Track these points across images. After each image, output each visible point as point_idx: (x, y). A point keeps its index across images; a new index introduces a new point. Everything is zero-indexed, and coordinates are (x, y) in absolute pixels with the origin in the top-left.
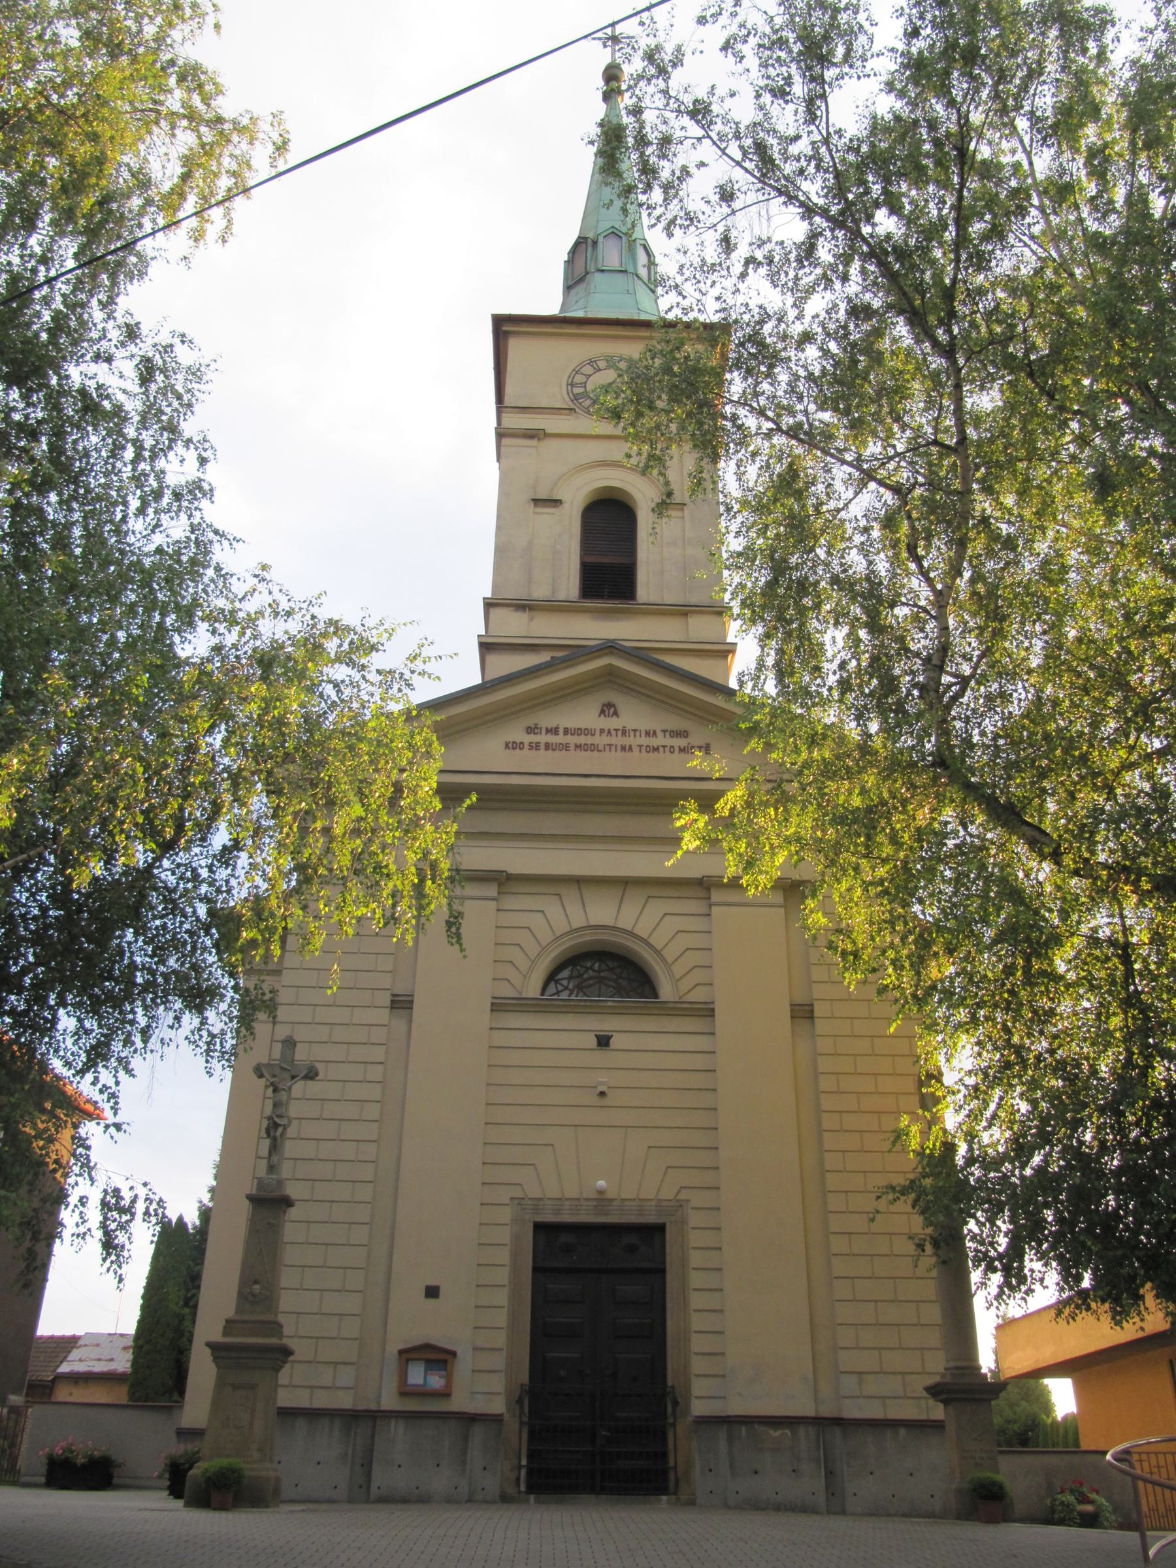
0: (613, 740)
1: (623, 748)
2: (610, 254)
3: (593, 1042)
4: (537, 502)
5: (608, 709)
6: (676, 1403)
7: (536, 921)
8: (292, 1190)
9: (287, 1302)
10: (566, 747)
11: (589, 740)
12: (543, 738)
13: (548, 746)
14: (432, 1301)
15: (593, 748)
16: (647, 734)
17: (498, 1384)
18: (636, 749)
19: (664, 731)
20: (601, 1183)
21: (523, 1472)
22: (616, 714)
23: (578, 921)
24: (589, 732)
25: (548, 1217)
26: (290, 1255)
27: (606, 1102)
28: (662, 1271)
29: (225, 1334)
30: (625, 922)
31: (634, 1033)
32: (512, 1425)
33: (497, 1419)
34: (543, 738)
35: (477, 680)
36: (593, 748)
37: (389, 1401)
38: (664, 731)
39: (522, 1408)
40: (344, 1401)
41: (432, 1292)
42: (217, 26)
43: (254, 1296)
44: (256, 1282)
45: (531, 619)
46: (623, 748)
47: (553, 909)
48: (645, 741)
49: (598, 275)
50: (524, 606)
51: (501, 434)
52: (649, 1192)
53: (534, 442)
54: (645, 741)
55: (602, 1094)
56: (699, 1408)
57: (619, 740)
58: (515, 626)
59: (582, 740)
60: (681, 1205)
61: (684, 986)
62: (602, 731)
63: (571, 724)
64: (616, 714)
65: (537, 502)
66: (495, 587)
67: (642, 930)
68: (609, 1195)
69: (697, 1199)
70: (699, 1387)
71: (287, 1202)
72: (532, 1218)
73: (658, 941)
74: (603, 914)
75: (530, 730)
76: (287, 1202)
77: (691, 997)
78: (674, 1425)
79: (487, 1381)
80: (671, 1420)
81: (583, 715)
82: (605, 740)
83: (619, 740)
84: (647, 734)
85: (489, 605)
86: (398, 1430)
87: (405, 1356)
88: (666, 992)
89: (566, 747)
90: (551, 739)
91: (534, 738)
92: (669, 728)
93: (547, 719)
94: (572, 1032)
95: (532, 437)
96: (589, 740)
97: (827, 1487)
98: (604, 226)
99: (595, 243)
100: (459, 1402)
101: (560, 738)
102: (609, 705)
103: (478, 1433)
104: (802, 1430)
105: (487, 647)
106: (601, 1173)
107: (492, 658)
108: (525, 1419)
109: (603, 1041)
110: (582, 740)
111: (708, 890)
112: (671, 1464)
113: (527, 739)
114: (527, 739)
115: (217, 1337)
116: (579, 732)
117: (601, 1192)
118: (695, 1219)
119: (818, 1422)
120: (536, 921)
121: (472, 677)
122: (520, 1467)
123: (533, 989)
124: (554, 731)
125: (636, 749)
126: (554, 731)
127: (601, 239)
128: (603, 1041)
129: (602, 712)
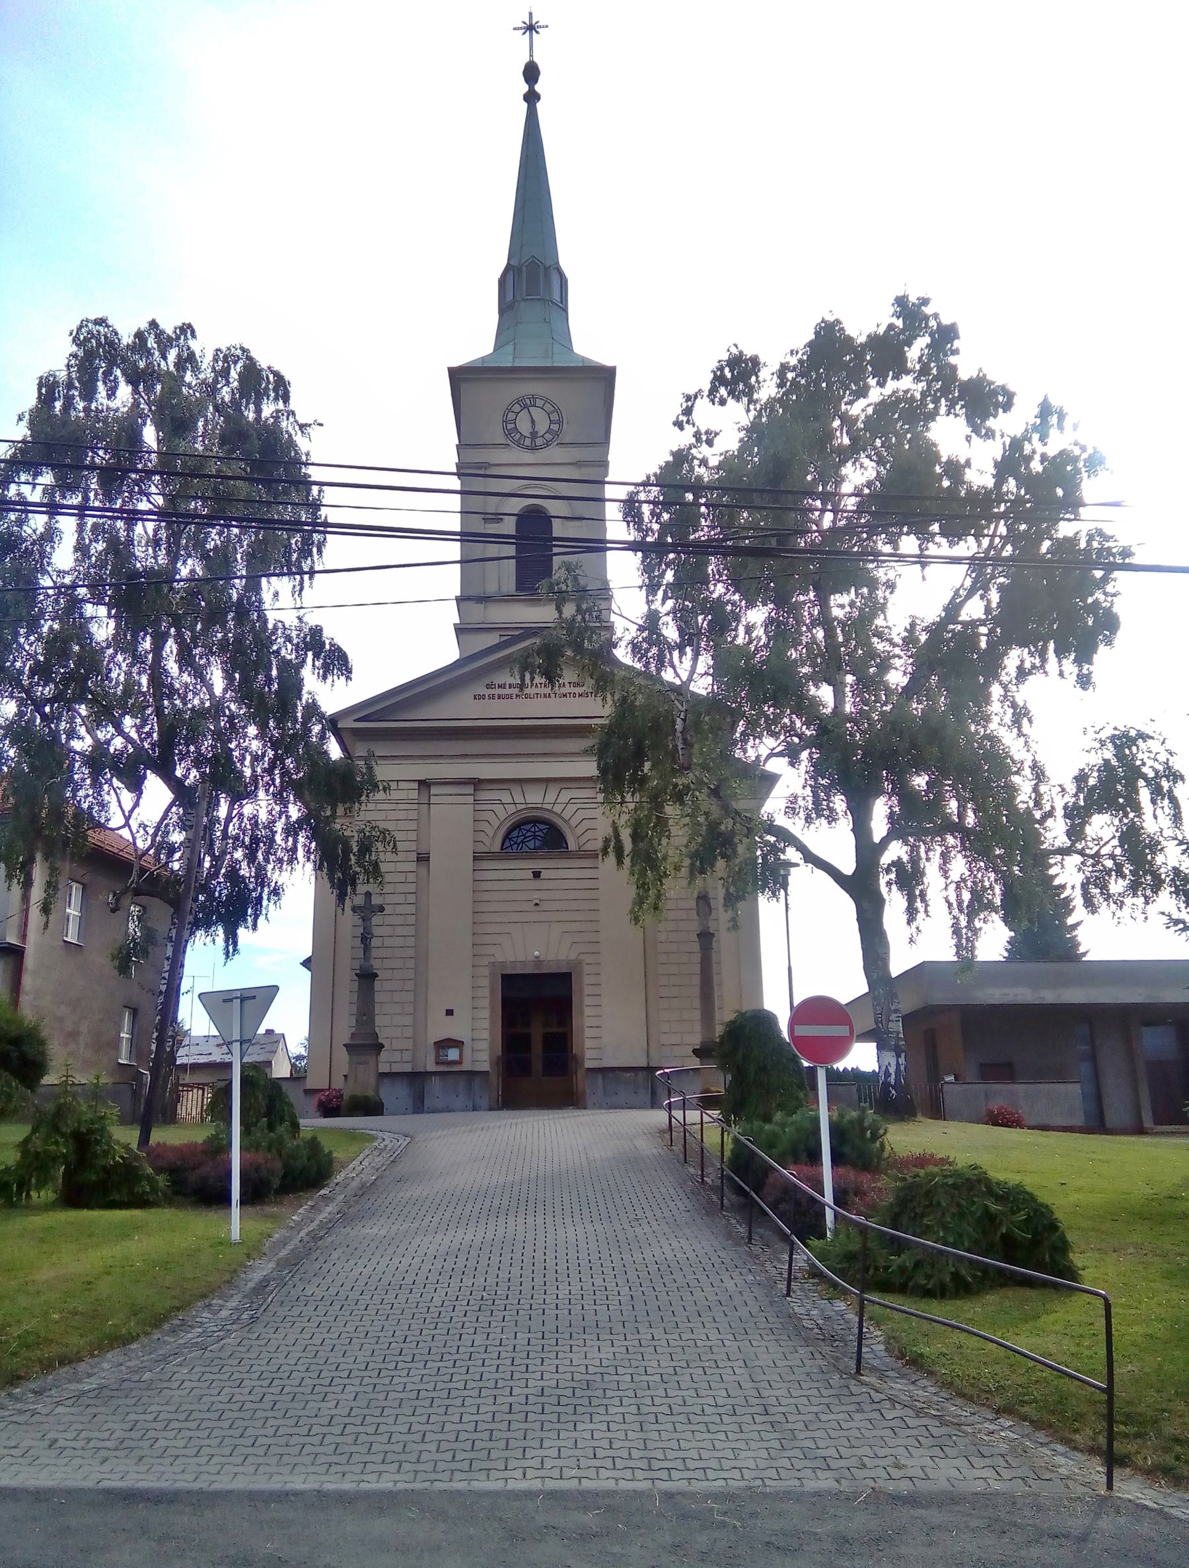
6: (577, 1063)
9: (379, 1021)
17: (485, 1056)
20: (537, 953)
25: (509, 972)
26: (378, 998)
31: (555, 870)
32: (495, 1079)
37: (431, 1067)
41: (450, 1013)
46: (545, 696)
50: (484, 599)
52: (562, 957)
55: (537, 904)
56: (589, 1064)
60: (579, 963)
61: (583, 840)
70: (589, 1054)
74: (534, 797)
75: (488, 687)
86: (436, 1082)
88: (572, 845)
91: (491, 691)
100: (466, 1066)
103: (477, 1082)
105: (460, 630)
106: (534, 947)
109: (537, 875)
123: (497, 847)
128: (537, 875)
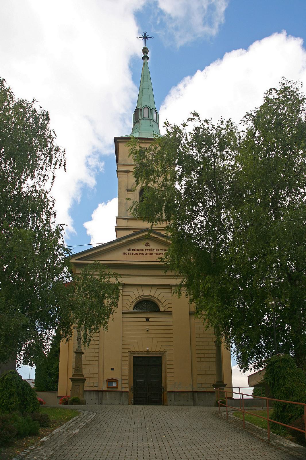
0: (148, 252)
1: (151, 254)
2: (145, 113)
3: (145, 320)
4: (128, 190)
5: (147, 244)
6: (164, 389)
7: (131, 294)
8: (83, 350)
9: (84, 371)
10: (137, 254)
11: (143, 252)
12: (132, 252)
13: (133, 254)
14: (112, 371)
15: (144, 254)
16: (157, 250)
17: (127, 386)
18: (154, 254)
19: (161, 250)
20: (147, 348)
21: (133, 401)
22: (149, 245)
23: (141, 294)
24: (142, 250)
25: (137, 355)
26: (83, 363)
27: (149, 332)
28: (160, 365)
29: (73, 376)
30: (152, 294)
31: (154, 319)
32: (130, 393)
33: (127, 392)
34: (132, 252)
35: (115, 238)
36: (144, 254)
37: (105, 389)
38: (161, 250)
39: (132, 390)
40: (96, 389)
41: (113, 369)
42: (56, 211)
43: (78, 370)
44: (78, 367)
45: (128, 222)
46: (151, 254)
47: (136, 291)
48: (156, 252)
49: (142, 120)
50: (126, 218)
51: (118, 171)
52: (158, 350)
53: (127, 174)
54: (156, 252)
55: (147, 331)
56: (168, 390)
57: (150, 252)
58: (124, 223)
59: (141, 252)
60: (165, 352)
61: (166, 308)
62: (146, 250)
63: (138, 248)
64: (149, 245)
65: (128, 190)
66: (119, 213)
67: (156, 296)
68: (150, 351)
69: (168, 351)
70: (168, 386)
71: (83, 353)
72: (133, 355)
73: (159, 298)
74: (147, 292)
75: (128, 250)
76: (83, 353)
77: (167, 310)
78: (163, 393)
79: (125, 384)
80: (163, 392)
81: (141, 246)
82: (147, 252)
83: (150, 252)
84: (157, 250)
85: (117, 218)
86: (107, 394)
87: (108, 381)
88: (162, 309)
89: (137, 254)
90: (134, 252)
91: (130, 252)
92: (162, 249)
93: (132, 247)
94: (141, 318)
95: (126, 172)
96: (143, 252)
97: (194, 403)
98: (144, 104)
99: (141, 110)
100: (119, 389)
101: (136, 252)
102: (147, 243)
103: (123, 394)
104: (189, 394)
105: (117, 229)
107: (118, 232)
108: (133, 392)
109: (148, 320)
110: (141, 252)
111: (171, 287)
112: (163, 399)
113: (128, 252)
114: (128, 252)
115: (71, 377)
116: (140, 250)
117: (148, 350)
118: (167, 355)
119: (193, 392)
120: (131, 294)
121: (114, 237)
122: (132, 400)
123: (132, 309)
124: (134, 250)
125: (154, 254)
126: (134, 250)
127: (143, 109)
128: (148, 320)
129: (146, 245)
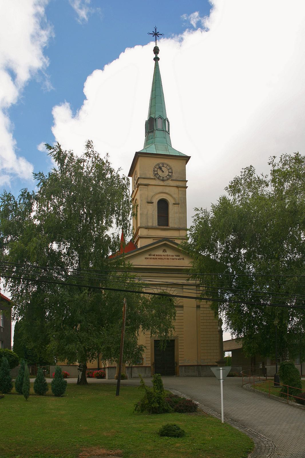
1: (167, 259)
5: (164, 251)
10: (157, 259)
11: (161, 257)
12: (152, 257)
15: (162, 259)
17: (150, 362)
18: (170, 259)
19: (175, 255)
22: (166, 252)
24: (161, 256)
32: (152, 367)
33: (150, 367)
34: (152, 257)
36: (162, 259)
38: (175, 255)
45: (148, 230)
46: (167, 259)
48: (171, 257)
54: (171, 257)
56: (180, 364)
57: (166, 257)
59: (160, 257)
62: (163, 255)
64: (166, 252)
70: (180, 362)
75: (150, 255)
81: (160, 252)
83: (166, 257)
84: (172, 256)
89: (157, 259)
91: (150, 257)
101: (155, 257)
110: (160, 257)
113: (149, 257)
116: (159, 255)
119: (198, 366)
124: (154, 255)
129: (163, 251)
